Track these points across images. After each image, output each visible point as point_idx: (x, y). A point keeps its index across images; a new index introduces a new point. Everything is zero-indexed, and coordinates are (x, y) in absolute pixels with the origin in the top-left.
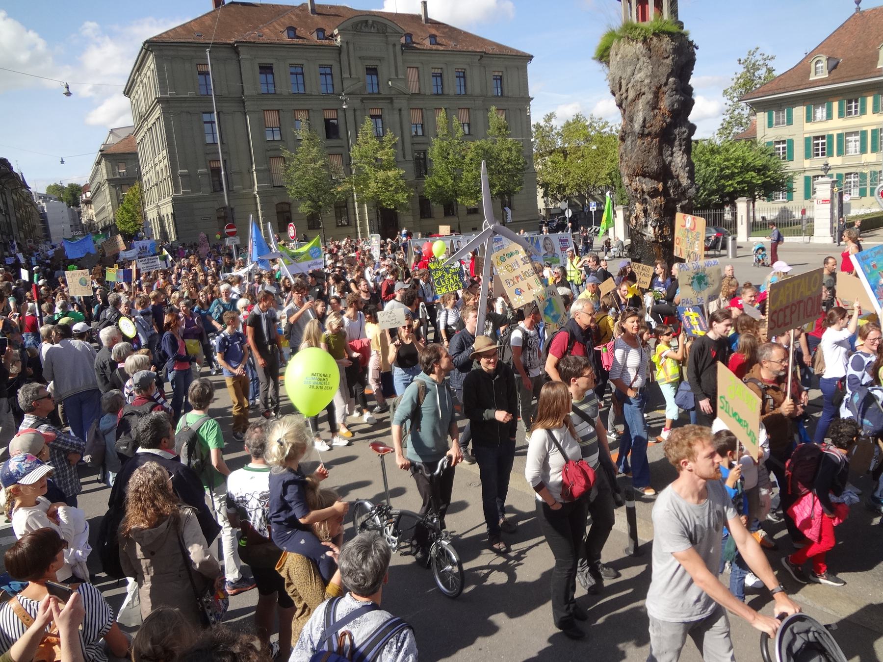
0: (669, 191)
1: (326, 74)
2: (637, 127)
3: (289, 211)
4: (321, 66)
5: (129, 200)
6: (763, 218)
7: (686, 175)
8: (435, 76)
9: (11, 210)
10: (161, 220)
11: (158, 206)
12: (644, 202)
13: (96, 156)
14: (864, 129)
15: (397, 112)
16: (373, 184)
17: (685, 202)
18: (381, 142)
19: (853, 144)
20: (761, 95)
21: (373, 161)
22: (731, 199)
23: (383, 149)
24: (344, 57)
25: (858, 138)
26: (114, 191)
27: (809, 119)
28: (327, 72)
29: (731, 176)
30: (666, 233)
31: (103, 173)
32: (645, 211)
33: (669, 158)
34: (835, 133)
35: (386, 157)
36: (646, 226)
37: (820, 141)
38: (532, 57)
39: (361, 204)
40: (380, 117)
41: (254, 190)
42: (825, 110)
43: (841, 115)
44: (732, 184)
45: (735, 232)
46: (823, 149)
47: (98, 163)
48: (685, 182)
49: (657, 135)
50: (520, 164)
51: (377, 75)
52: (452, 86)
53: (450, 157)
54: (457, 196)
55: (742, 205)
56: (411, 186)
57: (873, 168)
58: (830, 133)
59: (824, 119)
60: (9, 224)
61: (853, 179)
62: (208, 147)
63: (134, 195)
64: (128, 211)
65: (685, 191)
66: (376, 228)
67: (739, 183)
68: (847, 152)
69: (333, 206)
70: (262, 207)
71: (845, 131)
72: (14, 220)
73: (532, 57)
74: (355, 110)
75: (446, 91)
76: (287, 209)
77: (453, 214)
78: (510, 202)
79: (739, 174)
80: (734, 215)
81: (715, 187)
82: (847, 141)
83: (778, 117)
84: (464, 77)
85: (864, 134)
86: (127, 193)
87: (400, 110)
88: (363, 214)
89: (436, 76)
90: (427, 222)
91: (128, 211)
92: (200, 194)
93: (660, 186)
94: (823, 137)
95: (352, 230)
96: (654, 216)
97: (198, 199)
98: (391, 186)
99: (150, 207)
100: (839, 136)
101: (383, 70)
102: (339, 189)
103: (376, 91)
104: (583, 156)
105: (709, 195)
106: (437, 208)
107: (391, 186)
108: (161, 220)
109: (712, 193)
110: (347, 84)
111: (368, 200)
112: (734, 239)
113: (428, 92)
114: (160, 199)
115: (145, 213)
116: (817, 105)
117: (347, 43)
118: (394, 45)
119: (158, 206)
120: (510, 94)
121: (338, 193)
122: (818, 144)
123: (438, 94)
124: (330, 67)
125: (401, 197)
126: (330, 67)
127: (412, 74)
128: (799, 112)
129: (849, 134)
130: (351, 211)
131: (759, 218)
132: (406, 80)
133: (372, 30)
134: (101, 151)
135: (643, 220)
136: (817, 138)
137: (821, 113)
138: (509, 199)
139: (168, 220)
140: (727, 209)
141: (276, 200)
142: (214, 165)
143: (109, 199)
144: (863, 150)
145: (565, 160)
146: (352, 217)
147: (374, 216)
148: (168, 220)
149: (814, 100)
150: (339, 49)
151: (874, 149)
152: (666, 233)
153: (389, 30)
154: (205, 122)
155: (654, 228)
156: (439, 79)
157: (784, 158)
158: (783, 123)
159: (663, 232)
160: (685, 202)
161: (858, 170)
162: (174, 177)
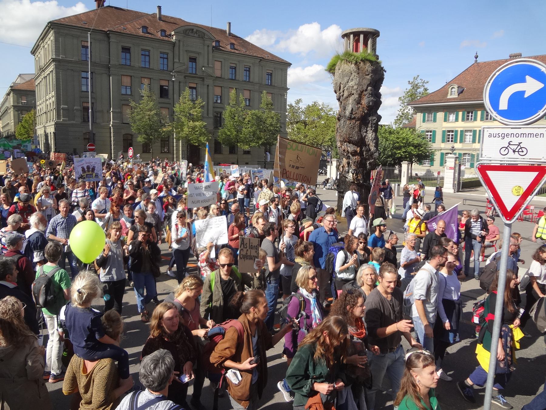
0: (363, 153)
1: (164, 58)
2: (348, 113)
3: (131, 140)
4: (161, 53)
5: (26, 121)
6: (416, 174)
7: (374, 145)
8: (231, 68)
10: (46, 136)
11: (45, 127)
12: (348, 158)
13: (7, 89)
14: (475, 129)
15: (206, 87)
16: (186, 129)
17: (371, 161)
18: (194, 104)
19: (469, 137)
20: (420, 103)
21: (188, 115)
22: (398, 162)
23: (195, 108)
24: (176, 48)
25: (471, 134)
26: (16, 113)
27: (446, 120)
28: (164, 57)
29: (399, 148)
30: (359, 178)
31: (11, 101)
32: (348, 163)
33: (365, 134)
34: (459, 130)
35: (196, 113)
36: (348, 172)
37: (451, 134)
38: (291, 64)
39: (178, 140)
40: (195, 88)
41: (110, 124)
42: (454, 116)
43: (463, 120)
44: (399, 153)
45: (400, 181)
46: (452, 138)
47: (8, 94)
48: (373, 149)
49: (358, 119)
50: (277, 127)
51: (196, 62)
52: (241, 75)
53: (236, 118)
54: (238, 142)
55: (405, 165)
56: (210, 133)
58: (457, 129)
61: (467, 157)
62: (83, 93)
63: (30, 118)
64: (24, 128)
65: (372, 154)
66: (186, 156)
67: (403, 152)
68: (465, 141)
69: (160, 139)
70: (114, 135)
73: (291, 64)
74: (180, 82)
75: (237, 78)
76: (130, 138)
77: (235, 153)
78: (270, 149)
79: (404, 147)
80: (400, 171)
81: (390, 153)
82: (466, 135)
83: (428, 117)
84: (249, 71)
85: (475, 132)
86: (26, 116)
87: (208, 86)
88: (179, 147)
89: (232, 68)
90: (217, 156)
91: (24, 128)
92: (74, 122)
93: (358, 149)
94: (452, 131)
95: (170, 156)
96: (353, 167)
97: (72, 125)
98: (197, 131)
99: (40, 126)
100: (461, 131)
101: (201, 61)
102: (164, 130)
103: (194, 72)
104: (316, 127)
105: (387, 158)
106: (225, 149)
107: (197, 131)
108: (46, 136)
109: (389, 157)
110: (176, 65)
111: (182, 138)
112: (399, 185)
113: (226, 77)
114: (47, 123)
115: (36, 130)
116: (451, 112)
117: (179, 41)
118: (208, 46)
119: (45, 127)
120: (276, 85)
121: (164, 132)
122: (449, 135)
123: (232, 79)
124: (167, 54)
125: (202, 139)
126: (167, 54)
127: (218, 65)
128: (440, 115)
129: (467, 131)
130: (171, 144)
131: (414, 174)
132: (213, 68)
133: (196, 35)
134: (11, 87)
135: (347, 169)
136: (449, 131)
137: (452, 117)
138: (270, 148)
139: (51, 136)
140: (397, 167)
141: (124, 132)
142: (85, 105)
144: (474, 141)
145: (305, 128)
146: (171, 148)
147: (185, 149)
148: (51, 136)
149: (449, 109)
150: (174, 44)
152: (359, 178)
153: (206, 37)
154: (83, 78)
155: (353, 174)
156: (234, 70)
157: (430, 141)
158: (431, 121)
159: (358, 177)
160: (371, 161)
161: (470, 152)
162: (58, 110)
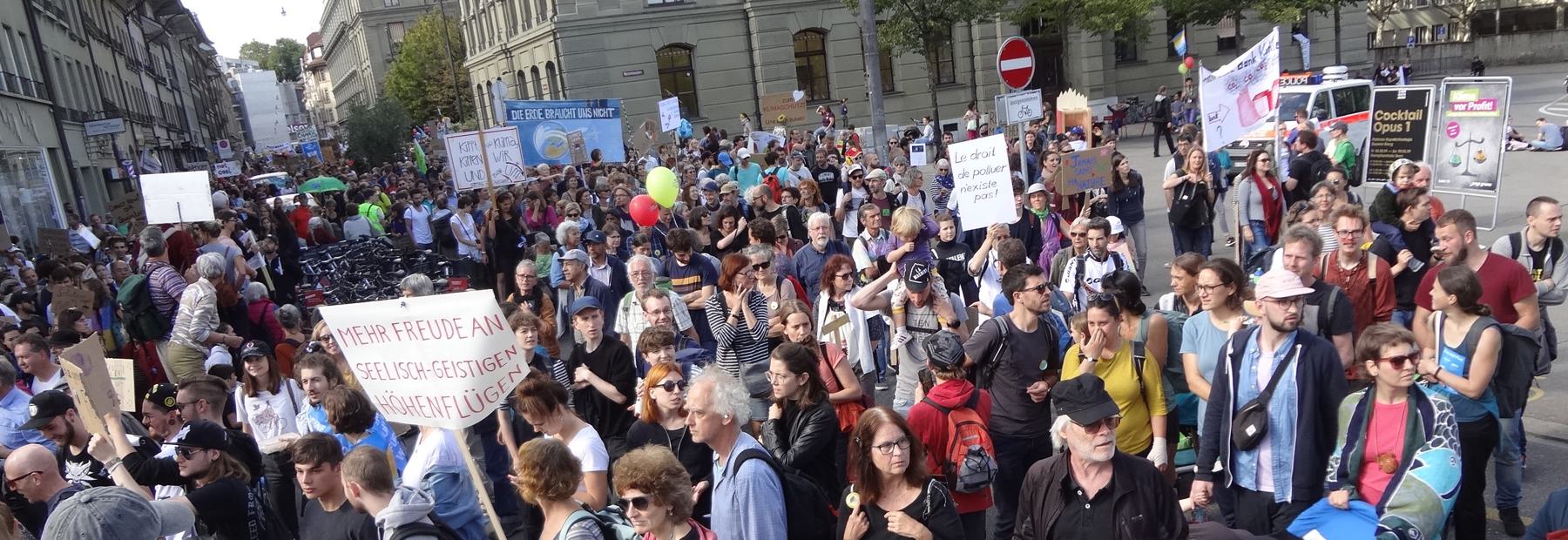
3: (823, 52)
9: (182, 82)
11: (507, 52)
60: (181, 110)
63: (419, 41)
72: (188, 103)
76: (819, 48)
90: (1130, 73)
95: (964, 96)
97: (618, 24)
99: (479, 56)
114: (513, 31)
119: (507, 52)
130: (960, 49)
141: (795, 23)
143: (364, 52)
146: (962, 64)
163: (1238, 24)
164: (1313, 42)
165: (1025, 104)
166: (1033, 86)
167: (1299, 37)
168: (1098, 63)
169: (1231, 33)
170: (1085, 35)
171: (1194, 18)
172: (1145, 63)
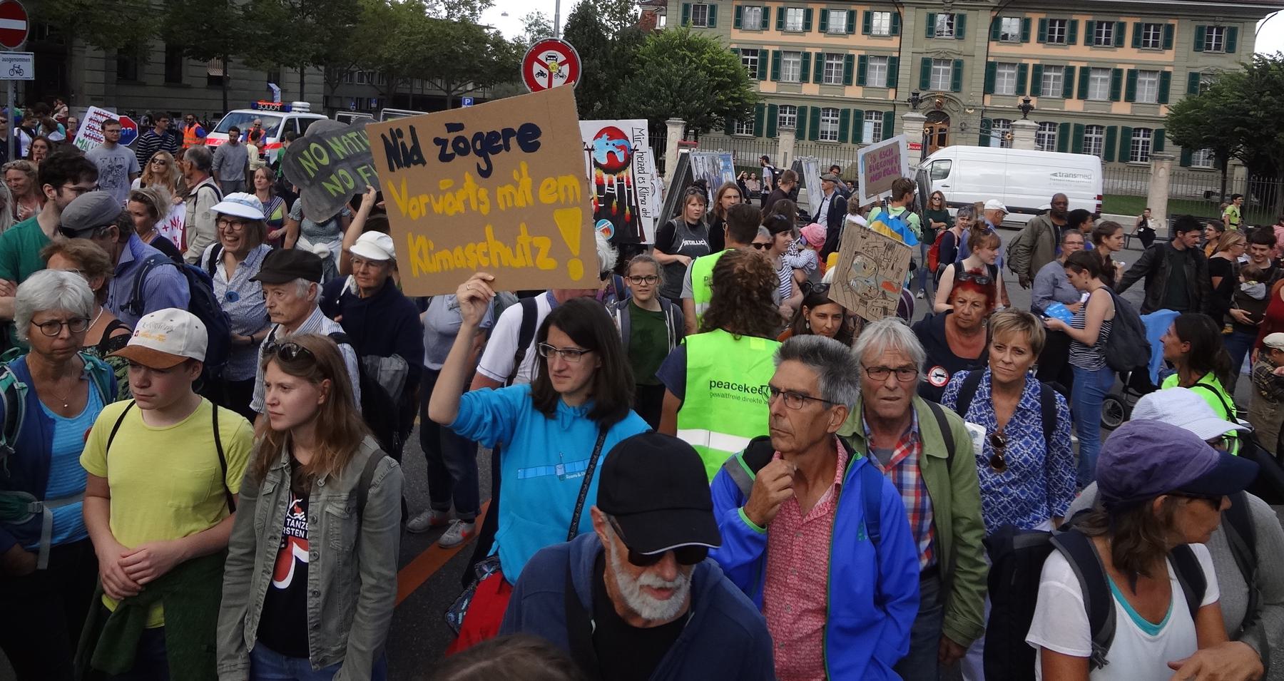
19: (791, 68)
25: (842, 62)
37: (750, 57)
46: (754, 68)
57: (859, 107)
58: (765, 48)
59: (800, 29)
61: (788, 115)
71: (783, 49)
94: (754, 52)
100: (819, 56)
122: (745, 61)
129: (830, 56)
136: (746, 52)
151: (818, 79)
157: (753, 75)
158: (703, 23)
163: (225, 64)
164: (283, 91)
165: (17, 64)
166: (28, 49)
167: (273, 86)
168: (100, 77)
169: (219, 73)
170: (90, 50)
171: (188, 54)
172: (144, 84)
